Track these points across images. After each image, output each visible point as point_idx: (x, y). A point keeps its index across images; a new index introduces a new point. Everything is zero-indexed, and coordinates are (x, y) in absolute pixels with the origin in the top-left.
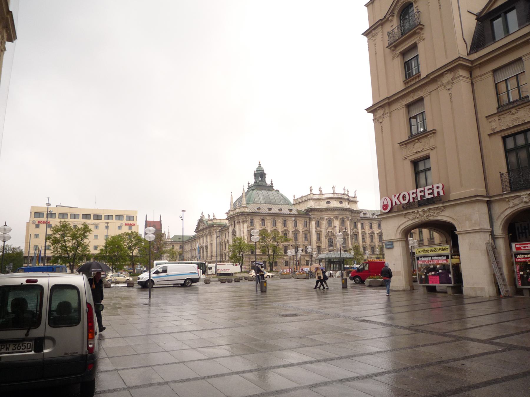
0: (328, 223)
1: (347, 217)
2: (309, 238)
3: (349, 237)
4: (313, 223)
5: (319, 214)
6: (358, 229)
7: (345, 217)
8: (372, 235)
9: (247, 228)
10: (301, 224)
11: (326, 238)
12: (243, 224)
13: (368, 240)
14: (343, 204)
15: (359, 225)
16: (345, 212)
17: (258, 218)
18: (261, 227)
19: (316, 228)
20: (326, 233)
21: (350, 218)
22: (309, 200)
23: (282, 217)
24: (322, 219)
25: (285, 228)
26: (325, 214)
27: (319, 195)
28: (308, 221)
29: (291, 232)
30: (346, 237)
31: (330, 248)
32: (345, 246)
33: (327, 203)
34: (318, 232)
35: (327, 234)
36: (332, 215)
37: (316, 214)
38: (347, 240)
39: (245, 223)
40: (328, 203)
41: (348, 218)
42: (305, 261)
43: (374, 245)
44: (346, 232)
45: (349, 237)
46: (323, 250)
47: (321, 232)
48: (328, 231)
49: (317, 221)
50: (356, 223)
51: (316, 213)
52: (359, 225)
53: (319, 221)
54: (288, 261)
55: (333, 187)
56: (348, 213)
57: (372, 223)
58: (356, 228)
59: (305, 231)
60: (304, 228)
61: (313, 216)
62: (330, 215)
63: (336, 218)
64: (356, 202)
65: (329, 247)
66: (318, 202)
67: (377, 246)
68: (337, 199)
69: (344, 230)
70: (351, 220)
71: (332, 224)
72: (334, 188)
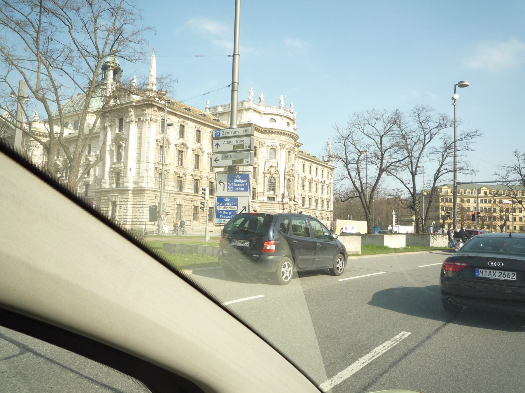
26: (267, 137)
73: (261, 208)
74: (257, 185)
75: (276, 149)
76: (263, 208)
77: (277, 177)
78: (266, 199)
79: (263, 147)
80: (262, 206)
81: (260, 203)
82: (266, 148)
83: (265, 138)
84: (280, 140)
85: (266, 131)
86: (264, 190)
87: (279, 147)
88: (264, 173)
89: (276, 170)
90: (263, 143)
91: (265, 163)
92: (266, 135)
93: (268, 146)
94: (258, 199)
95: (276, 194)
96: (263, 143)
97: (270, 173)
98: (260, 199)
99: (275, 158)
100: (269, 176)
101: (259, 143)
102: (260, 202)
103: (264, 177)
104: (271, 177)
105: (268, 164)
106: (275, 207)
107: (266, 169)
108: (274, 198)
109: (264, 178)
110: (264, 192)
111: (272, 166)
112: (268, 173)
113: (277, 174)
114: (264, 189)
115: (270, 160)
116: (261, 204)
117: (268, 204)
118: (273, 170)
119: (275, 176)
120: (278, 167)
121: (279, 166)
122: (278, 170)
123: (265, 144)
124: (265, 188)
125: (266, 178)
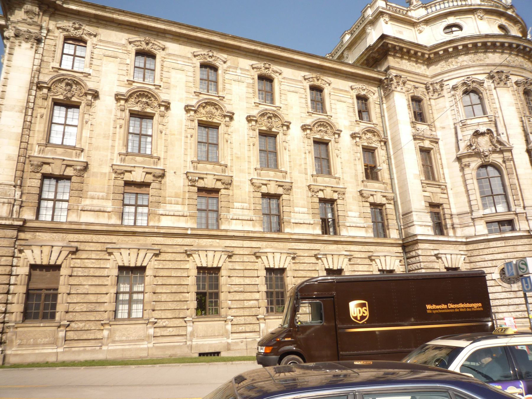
25: (267, 107)
73: (473, 259)
74: (445, 196)
75: (481, 89)
76: (478, 258)
77: (504, 162)
78: (481, 229)
79: (440, 96)
80: (476, 253)
81: (467, 243)
82: (450, 95)
83: (439, 71)
86: (470, 206)
87: (488, 84)
88: (459, 159)
89: (495, 140)
90: (438, 87)
91: (456, 133)
92: (442, 63)
93: (454, 88)
94: (455, 232)
95: (513, 208)
96: (438, 87)
97: (478, 154)
98: (462, 233)
99: (484, 112)
100: (475, 162)
101: (427, 88)
102: (464, 240)
103: (462, 169)
104: (484, 166)
105: (465, 133)
106: (520, 248)
107: (462, 145)
108: (510, 222)
109: (461, 174)
110: (472, 212)
111: (477, 134)
112: (470, 156)
113: (501, 152)
114: (469, 201)
115: (469, 122)
116: (471, 247)
117: (492, 244)
118: (484, 143)
119: (497, 158)
120: (500, 132)
121: (501, 129)
122: (503, 138)
123: (445, 88)
124: (472, 198)
125: (467, 171)
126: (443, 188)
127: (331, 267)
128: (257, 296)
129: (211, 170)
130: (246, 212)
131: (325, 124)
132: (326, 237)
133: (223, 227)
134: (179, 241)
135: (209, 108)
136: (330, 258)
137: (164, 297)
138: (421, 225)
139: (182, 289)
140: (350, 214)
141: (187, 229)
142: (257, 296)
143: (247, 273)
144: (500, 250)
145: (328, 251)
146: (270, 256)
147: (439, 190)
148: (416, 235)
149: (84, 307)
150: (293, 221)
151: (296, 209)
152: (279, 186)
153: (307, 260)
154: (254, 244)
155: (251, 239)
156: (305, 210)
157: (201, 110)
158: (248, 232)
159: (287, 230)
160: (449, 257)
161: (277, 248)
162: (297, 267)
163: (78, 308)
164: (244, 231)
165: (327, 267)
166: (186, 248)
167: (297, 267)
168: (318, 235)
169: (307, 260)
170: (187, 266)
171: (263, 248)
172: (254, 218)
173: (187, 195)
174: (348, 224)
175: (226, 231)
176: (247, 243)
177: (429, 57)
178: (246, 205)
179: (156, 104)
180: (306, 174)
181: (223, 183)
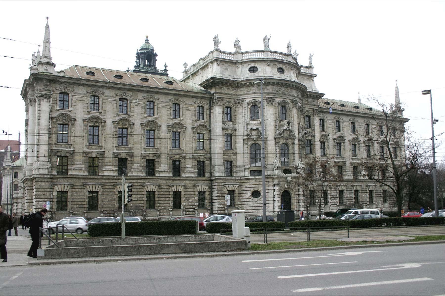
0: (250, 111)
1: (293, 101)
2: (208, 142)
3: (297, 142)
4: (218, 111)
5: (231, 92)
6: (313, 130)
7: (289, 101)
8: (340, 141)
9: (51, 111)
10: (190, 112)
11: (245, 144)
12: (40, 102)
13: (331, 151)
14: (285, 74)
15: (317, 122)
16: (289, 90)
17: (80, 91)
18: (89, 113)
19: (224, 122)
20: (246, 133)
21: (299, 104)
22: (212, 63)
23: (145, 95)
24: (239, 102)
25: (151, 118)
26: (246, 92)
27: (233, 54)
28: (206, 107)
29: (164, 128)
30: (290, 142)
31: (254, 165)
32: (286, 160)
33: (249, 70)
34: (227, 129)
35: (248, 135)
36: (259, 95)
37: (227, 92)
38: (290, 148)
39: (45, 100)
40: (253, 69)
41: (294, 102)
42: (197, 193)
43: (343, 163)
44: (290, 130)
45: (297, 142)
46: (238, 169)
47: (235, 130)
48: (250, 127)
49: (227, 107)
50: (309, 117)
51: (225, 90)
52: (317, 122)
53: (231, 108)
54: (154, 192)
55: (264, 39)
56: (294, 93)
57: (341, 121)
58: (310, 127)
59: (198, 126)
60: (196, 121)
61: (216, 96)
62: (255, 95)
63: (270, 101)
64: (312, 77)
65: (251, 163)
66: (230, 68)
67: (348, 164)
68: (272, 63)
69: (285, 127)
70: (301, 110)
71: (260, 112)
72: (266, 40)
74: (235, 157)
84: (265, 93)
85: (242, 84)
90: (241, 102)
101: (235, 102)
126: (235, 154)
127: (176, 190)
128: (142, 202)
129: (124, 150)
130: (139, 167)
131: (179, 125)
132: (174, 178)
133: (129, 175)
134: (111, 181)
135: (124, 121)
136: (175, 187)
137: (106, 203)
138: (219, 172)
139: (113, 199)
140: (187, 166)
141: (114, 176)
142: (142, 202)
143: (139, 193)
144: (253, 183)
145: (175, 183)
146: (149, 186)
147: (232, 155)
148: (216, 177)
149: (77, 206)
150: (160, 171)
151: (162, 165)
152: (154, 155)
153: (165, 187)
154: (142, 181)
155: (141, 179)
156: (166, 165)
157: (120, 123)
158: (140, 176)
159: (157, 175)
160: (230, 186)
161: (152, 183)
162: (160, 190)
163: (75, 206)
164: (138, 176)
165: (174, 190)
166: (114, 184)
167: (160, 190)
168: (171, 177)
169: (165, 187)
170: (114, 191)
171: (146, 183)
172: (142, 170)
173: (114, 161)
174: (185, 171)
175: (130, 176)
176: (139, 181)
177: (238, 85)
178: (139, 164)
179: (100, 122)
180: (168, 149)
181: (129, 156)
